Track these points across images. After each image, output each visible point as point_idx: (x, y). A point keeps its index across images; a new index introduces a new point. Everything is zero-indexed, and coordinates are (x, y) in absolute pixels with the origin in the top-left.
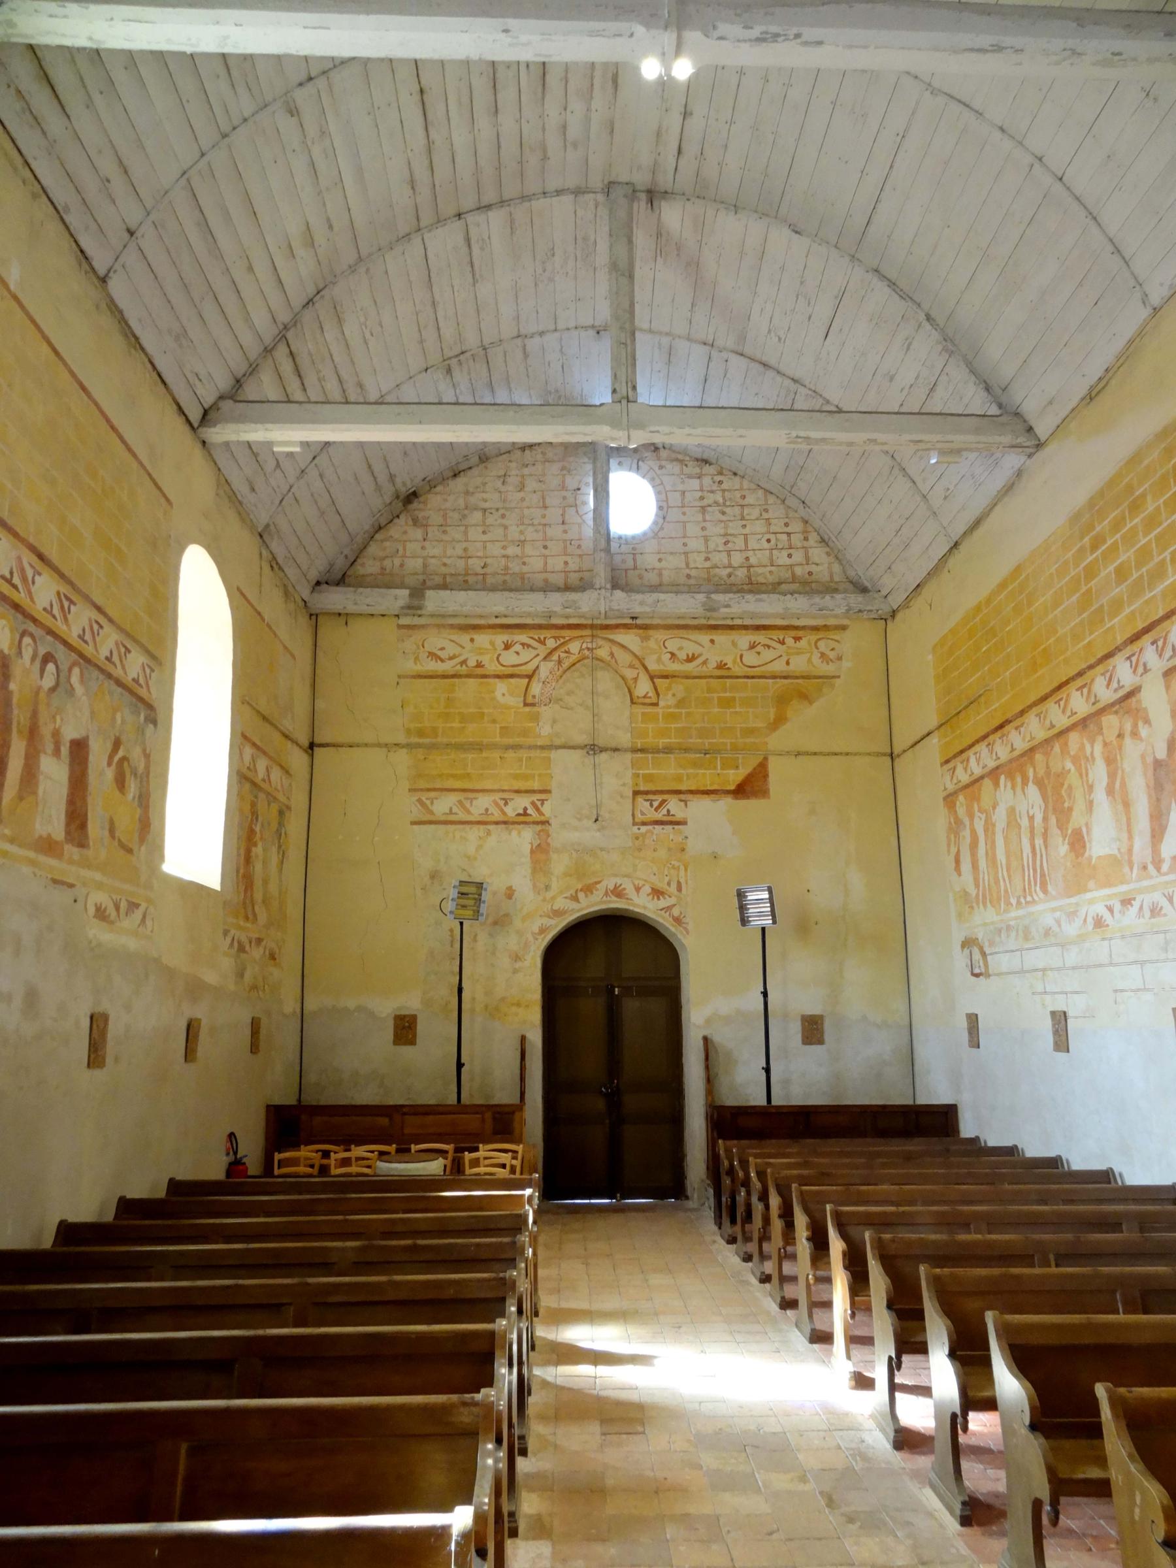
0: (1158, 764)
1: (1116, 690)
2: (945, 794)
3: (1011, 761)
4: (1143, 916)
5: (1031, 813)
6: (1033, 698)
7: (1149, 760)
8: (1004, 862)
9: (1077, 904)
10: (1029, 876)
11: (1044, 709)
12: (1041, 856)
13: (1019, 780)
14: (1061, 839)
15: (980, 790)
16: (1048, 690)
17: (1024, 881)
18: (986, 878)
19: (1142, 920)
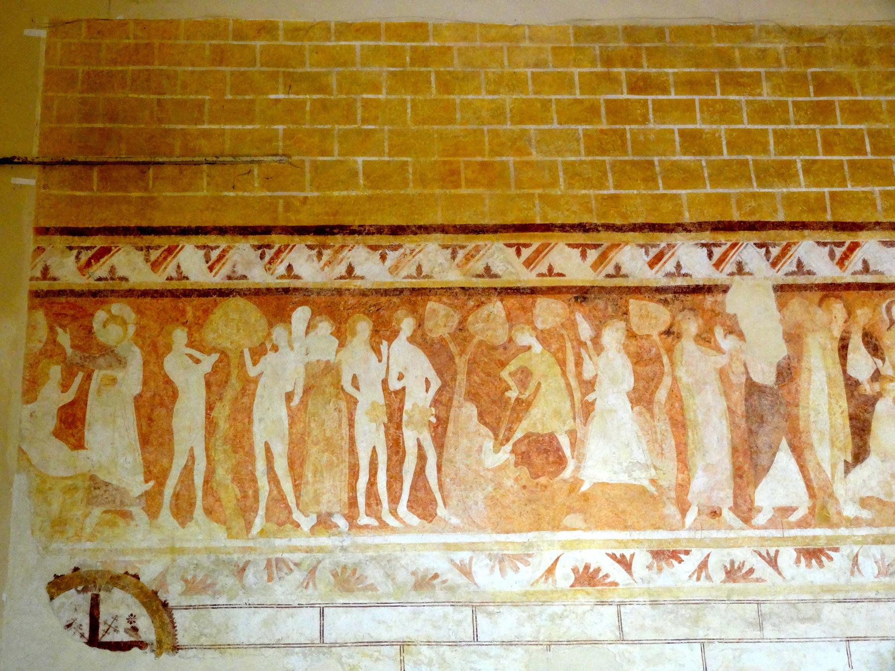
0: (753, 389)
1: (669, 275)
2: (44, 285)
3: (339, 292)
4: (708, 578)
5: (395, 385)
6: (438, 219)
7: (739, 379)
8: (280, 450)
9: (529, 545)
10: (372, 483)
11: (471, 246)
12: (422, 457)
13: (364, 327)
14: (489, 444)
15: (207, 312)
16: (487, 221)
17: (353, 488)
18: (200, 466)
19: (703, 582)
